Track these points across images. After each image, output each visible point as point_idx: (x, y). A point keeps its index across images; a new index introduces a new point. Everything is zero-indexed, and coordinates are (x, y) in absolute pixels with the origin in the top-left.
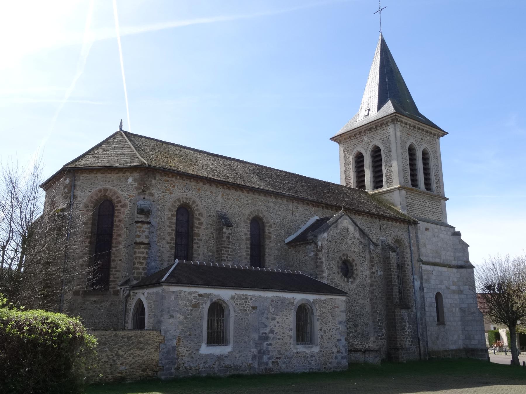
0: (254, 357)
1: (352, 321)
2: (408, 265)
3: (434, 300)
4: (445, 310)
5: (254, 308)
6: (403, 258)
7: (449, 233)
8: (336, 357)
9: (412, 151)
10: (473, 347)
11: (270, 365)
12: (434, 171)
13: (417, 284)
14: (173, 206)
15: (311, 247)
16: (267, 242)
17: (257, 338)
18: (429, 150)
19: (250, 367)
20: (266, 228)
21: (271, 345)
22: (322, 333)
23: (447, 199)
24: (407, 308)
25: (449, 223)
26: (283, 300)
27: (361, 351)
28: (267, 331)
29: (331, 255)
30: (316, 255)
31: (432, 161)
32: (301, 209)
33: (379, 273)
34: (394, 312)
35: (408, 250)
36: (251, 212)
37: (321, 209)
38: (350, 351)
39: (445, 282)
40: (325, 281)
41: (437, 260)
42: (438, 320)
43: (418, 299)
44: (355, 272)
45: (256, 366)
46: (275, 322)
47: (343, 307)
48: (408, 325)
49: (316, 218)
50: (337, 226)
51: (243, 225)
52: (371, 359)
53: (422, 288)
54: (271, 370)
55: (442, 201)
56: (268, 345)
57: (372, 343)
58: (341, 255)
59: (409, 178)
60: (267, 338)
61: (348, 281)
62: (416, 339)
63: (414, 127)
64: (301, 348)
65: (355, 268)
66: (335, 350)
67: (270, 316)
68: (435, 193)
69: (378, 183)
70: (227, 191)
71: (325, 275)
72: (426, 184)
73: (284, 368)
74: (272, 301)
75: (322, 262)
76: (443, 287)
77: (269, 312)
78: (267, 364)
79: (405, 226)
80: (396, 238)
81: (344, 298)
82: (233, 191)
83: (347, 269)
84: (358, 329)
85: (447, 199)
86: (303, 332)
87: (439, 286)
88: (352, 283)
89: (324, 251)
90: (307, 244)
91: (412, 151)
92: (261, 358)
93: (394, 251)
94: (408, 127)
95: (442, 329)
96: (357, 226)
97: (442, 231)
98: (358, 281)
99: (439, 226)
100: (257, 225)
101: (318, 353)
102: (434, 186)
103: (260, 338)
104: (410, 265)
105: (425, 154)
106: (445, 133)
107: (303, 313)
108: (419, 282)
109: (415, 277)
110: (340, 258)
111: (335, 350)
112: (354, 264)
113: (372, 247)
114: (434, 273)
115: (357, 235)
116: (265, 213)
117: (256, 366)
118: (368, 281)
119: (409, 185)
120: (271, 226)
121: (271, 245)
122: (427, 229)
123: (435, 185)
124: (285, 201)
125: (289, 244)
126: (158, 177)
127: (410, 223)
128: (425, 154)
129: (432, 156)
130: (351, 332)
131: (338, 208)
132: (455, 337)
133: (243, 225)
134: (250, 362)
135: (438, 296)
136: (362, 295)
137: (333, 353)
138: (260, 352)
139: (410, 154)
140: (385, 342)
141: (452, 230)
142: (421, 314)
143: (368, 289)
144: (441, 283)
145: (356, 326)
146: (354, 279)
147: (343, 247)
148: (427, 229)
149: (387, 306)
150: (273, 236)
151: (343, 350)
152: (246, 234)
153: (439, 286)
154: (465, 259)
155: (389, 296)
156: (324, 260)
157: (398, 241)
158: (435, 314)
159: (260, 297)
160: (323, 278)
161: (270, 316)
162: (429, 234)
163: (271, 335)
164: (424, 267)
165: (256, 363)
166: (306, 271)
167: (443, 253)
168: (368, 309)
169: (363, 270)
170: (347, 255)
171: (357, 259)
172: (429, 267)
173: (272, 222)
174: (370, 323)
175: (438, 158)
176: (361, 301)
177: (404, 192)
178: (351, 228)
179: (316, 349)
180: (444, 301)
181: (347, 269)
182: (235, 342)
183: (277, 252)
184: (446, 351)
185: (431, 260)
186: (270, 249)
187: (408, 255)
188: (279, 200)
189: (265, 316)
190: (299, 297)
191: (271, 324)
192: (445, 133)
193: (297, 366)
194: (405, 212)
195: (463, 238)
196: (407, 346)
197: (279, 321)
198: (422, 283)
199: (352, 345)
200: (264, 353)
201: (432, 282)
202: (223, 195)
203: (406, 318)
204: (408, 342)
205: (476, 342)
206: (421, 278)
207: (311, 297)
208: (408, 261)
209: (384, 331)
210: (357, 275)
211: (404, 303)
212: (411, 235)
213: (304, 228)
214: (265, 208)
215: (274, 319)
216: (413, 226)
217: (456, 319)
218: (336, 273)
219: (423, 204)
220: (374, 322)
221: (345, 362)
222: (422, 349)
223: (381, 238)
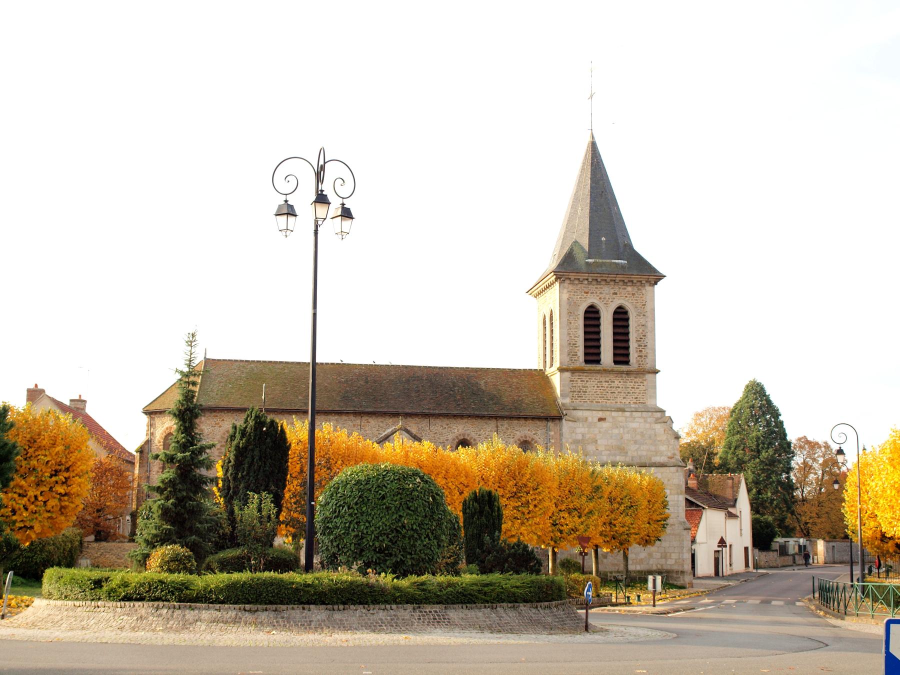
9: (592, 316)
10: (669, 568)
12: (635, 335)
14: (222, 438)
25: (660, 404)
91: (592, 316)
94: (586, 282)
97: (634, 418)
99: (628, 414)
122: (600, 420)
123: (636, 355)
124: (352, 417)
126: (208, 414)
129: (635, 314)
141: (658, 415)
148: (600, 420)
162: (604, 424)
175: (647, 313)
194: (560, 401)
216: (557, 421)
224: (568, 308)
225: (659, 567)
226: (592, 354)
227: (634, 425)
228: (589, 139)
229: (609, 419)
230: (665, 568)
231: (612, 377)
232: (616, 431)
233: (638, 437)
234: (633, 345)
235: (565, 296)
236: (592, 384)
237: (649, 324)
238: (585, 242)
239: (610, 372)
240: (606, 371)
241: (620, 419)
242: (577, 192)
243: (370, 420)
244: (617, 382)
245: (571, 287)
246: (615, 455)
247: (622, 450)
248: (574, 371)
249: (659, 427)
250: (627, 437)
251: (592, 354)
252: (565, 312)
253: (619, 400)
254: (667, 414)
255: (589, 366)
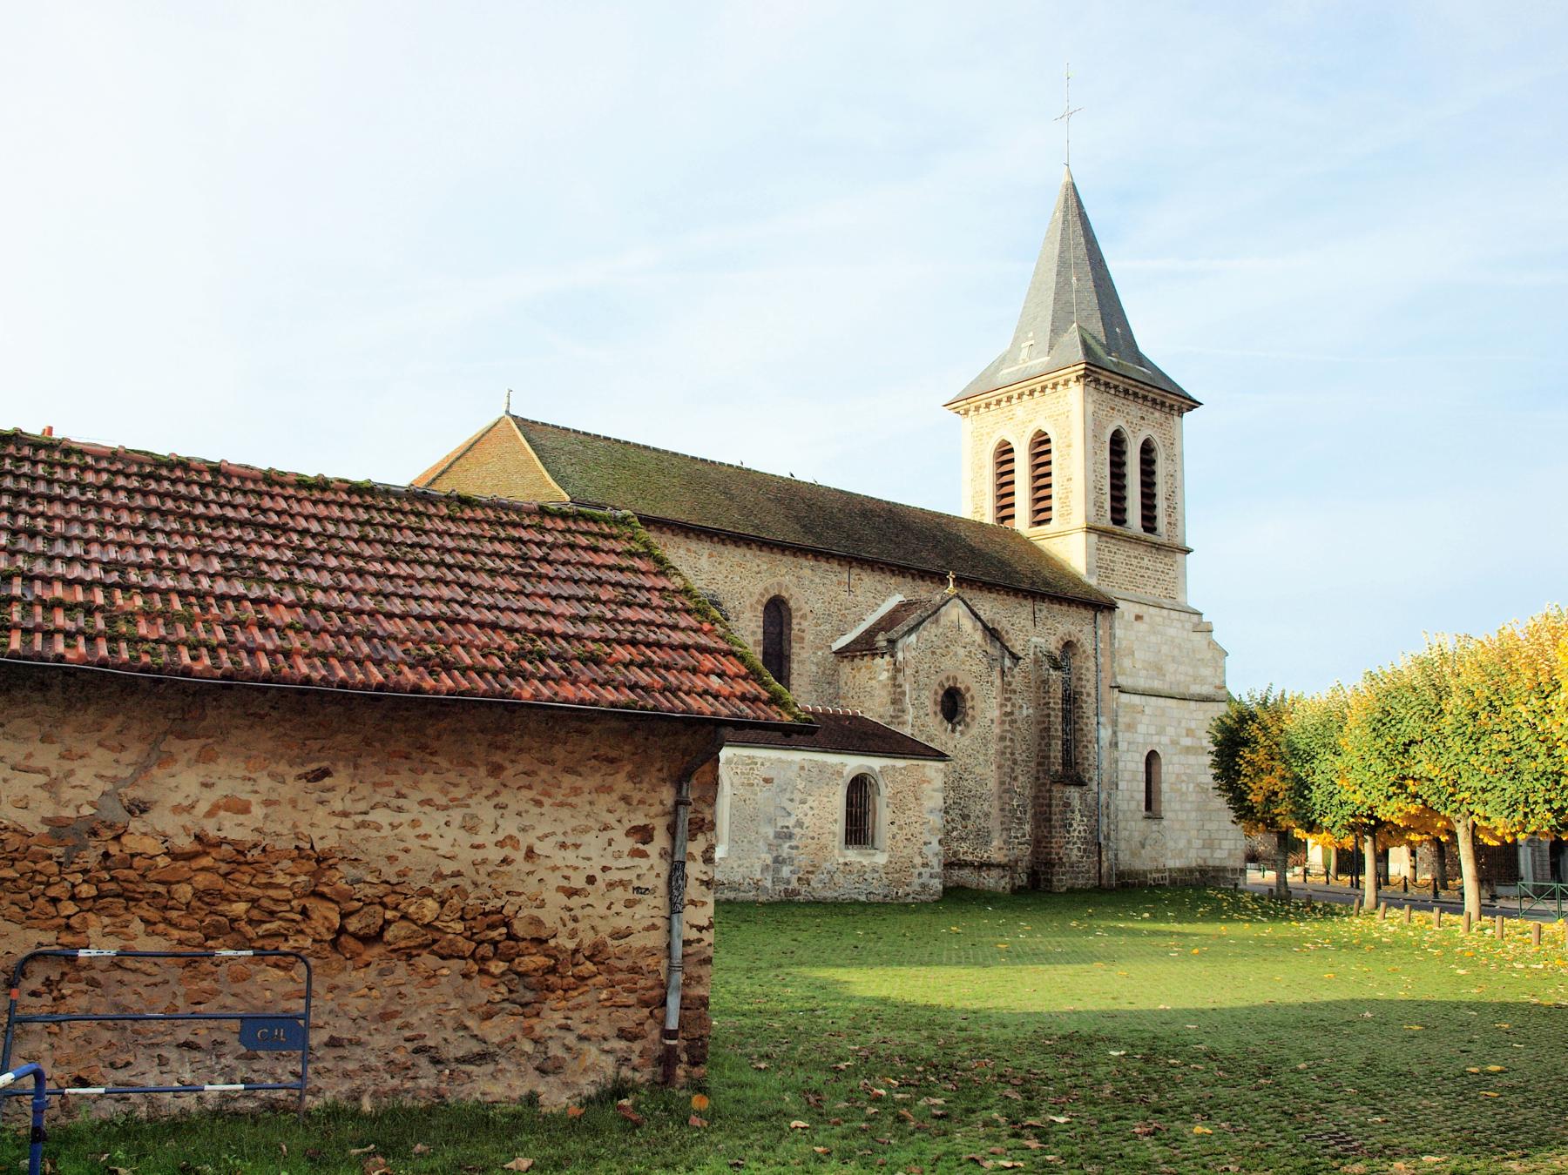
0: (765, 868)
1: (957, 809)
2: (1089, 695)
3: (1142, 768)
4: (1165, 787)
5: (767, 781)
6: (1080, 679)
7: (1189, 626)
8: (920, 874)
9: (1117, 443)
10: (1217, 863)
11: (794, 884)
13: (1105, 734)
15: (882, 663)
16: (795, 648)
17: (771, 835)
18: (1158, 443)
19: (757, 886)
20: (794, 621)
21: (797, 847)
22: (894, 828)
23: (1188, 551)
24: (1080, 783)
25: (1193, 602)
26: (822, 768)
27: (972, 864)
28: (791, 822)
29: (922, 679)
30: (894, 678)
31: (1161, 468)
32: (867, 582)
33: (1025, 712)
34: (1050, 791)
35: (1091, 664)
36: (766, 589)
37: (909, 579)
38: (949, 865)
39: (1170, 731)
40: (907, 731)
41: (1157, 685)
42: (1148, 806)
43: (1105, 765)
44: (970, 712)
45: (769, 884)
46: (806, 807)
47: (938, 781)
48: (1078, 817)
49: (896, 599)
50: (937, 621)
51: (748, 615)
52: (991, 881)
53: (1114, 745)
54: (796, 893)
55: (1179, 556)
56: (791, 848)
57: (995, 851)
58: (942, 677)
59: (1107, 506)
60: (790, 836)
61: (953, 731)
62: (1095, 845)
63: (1126, 392)
64: (853, 855)
65: (969, 704)
66: (918, 860)
67: (797, 796)
68: (1164, 539)
69: (1041, 514)
70: (720, 547)
71: (909, 718)
72: (1144, 518)
73: (819, 888)
74: (802, 768)
75: (904, 693)
76: (1165, 740)
77: (795, 787)
78: (788, 882)
79: (1090, 614)
80: (1067, 638)
81: (941, 765)
82: (731, 547)
83: (952, 704)
84: (969, 824)
85: (1188, 551)
86: (858, 829)
87: (1156, 739)
88: (962, 733)
89: (908, 671)
90: (874, 655)
91: (1117, 442)
92: (777, 871)
93: (1057, 667)
95: (1155, 828)
96: (980, 619)
98: (975, 730)
100: (777, 611)
101: (885, 867)
102: (1162, 522)
103: (778, 836)
104: (1093, 692)
105: (1147, 450)
106: (1194, 404)
107: (859, 788)
108: (1110, 731)
109: (1102, 719)
110: (941, 685)
111: (918, 860)
112: (968, 696)
113: (1008, 663)
114: (1147, 710)
115: (978, 637)
116: (794, 590)
117: (769, 884)
118: (997, 730)
119: (1106, 522)
120: (804, 617)
121: (804, 655)
122: (1138, 618)
123: (1166, 520)
125: (842, 653)
127: (1102, 606)
128: (1147, 450)
130: (954, 829)
131: (943, 580)
132: (1182, 844)
133: (748, 615)
134: (759, 877)
135: (1152, 757)
136: (981, 758)
137: (914, 867)
138: (776, 860)
139: (1112, 452)
140: (1026, 850)
142: (1109, 795)
143: (994, 747)
144: (1161, 731)
145: (965, 817)
146: (967, 725)
147: (947, 664)
148: (1138, 618)
149: (1038, 779)
150: (809, 637)
151: (934, 862)
152: (753, 633)
153: (1156, 739)
154: (1217, 682)
155: (1043, 760)
156: (907, 687)
157: (1069, 646)
158: (1143, 795)
159: (780, 761)
160: (904, 723)
161: (797, 796)
162: (1142, 627)
163: (797, 830)
164: (1124, 698)
165: (770, 878)
166: (875, 709)
167: (1171, 667)
168: (992, 784)
169: (986, 707)
170: (955, 678)
171: (974, 687)
172: (1136, 699)
173: (806, 609)
174: (995, 812)
176: (978, 770)
177: (1094, 537)
178: (968, 624)
179: (881, 859)
180: (1164, 769)
181: (952, 704)
182: (732, 840)
183: (814, 668)
184: (1157, 871)
185: (1142, 683)
186: (802, 662)
187: (1091, 676)
188: (824, 565)
189: (788, 795)
190: (854, 764)
191: (798, 811)
192: (1194, 404)
193: (846, 888)
194: (1093, 582)
195: (1215, 636)
196: (1074, 858)
197: (814, 805)
198: (1115, 733)
199: (955, 853)
200: (784, 862)
201: (1141, 728)
202: (711, 556)
203: (1076, 803)
204: (1075, 851)
205: (1224, 854)
206: (1115, 723)
207: (874, 763)
208: (1089, 687)
209: (1027, 828)
210: (973, 718)
211: (1073, 774)
212: (1100, 632)
213: (871, 619)
214: (794, 579)
215: (803, 802)
216: (1106, 613)
217: (1188, 806)
218: (932, 715)
219: (1134, 561)
220: (1002, 810)
221: (937, 885)
222: (1105, 865)
223: (1034, 639)
224: (1093, 426)
225: (1201, 862)
226: (1118, 514)
227: (1172, 632)
228: (1065, 179)
229: (1146, 618)
230: (1210, 863)
231: (1141, 550)
232: (1153, 639)
233: (1176, 652)
234: (1161, 504)
235: (1091, 408)
236: (1121, 555)
237: (1178, 475)
238: (1097, 327)
239: (1137, 540)
240: (1137, 540)
241: (1159, 620)
242: (1061, 252)
243: (864, 575)
244: (1145, 562)
245: (1096, 396)
246: (1152, 678)
247: (1159, 670)
248: (1102, 533)
249: (1197, 636)
250: (1165, 649)
251: (1118, 514)
252: (1090, 434)
253: (1149, 589)
254: (1205, 619)
255: (1117, 529)
